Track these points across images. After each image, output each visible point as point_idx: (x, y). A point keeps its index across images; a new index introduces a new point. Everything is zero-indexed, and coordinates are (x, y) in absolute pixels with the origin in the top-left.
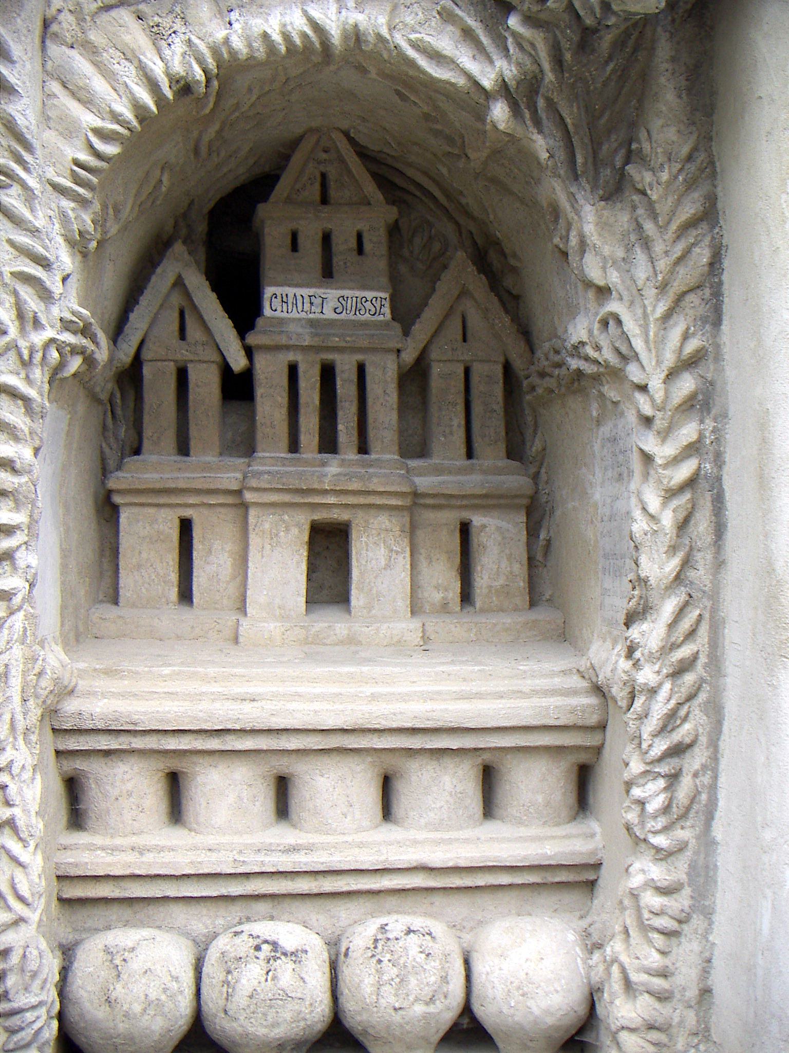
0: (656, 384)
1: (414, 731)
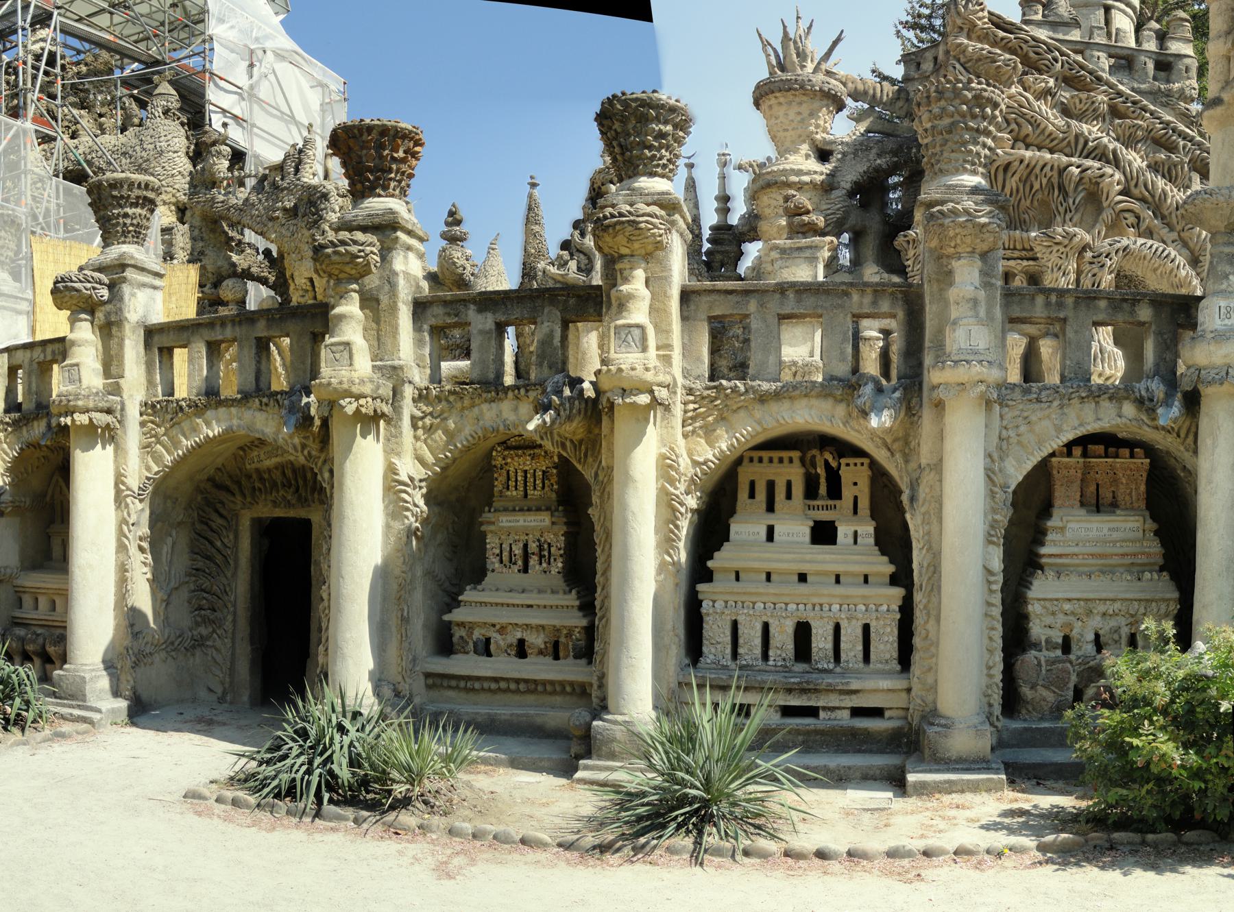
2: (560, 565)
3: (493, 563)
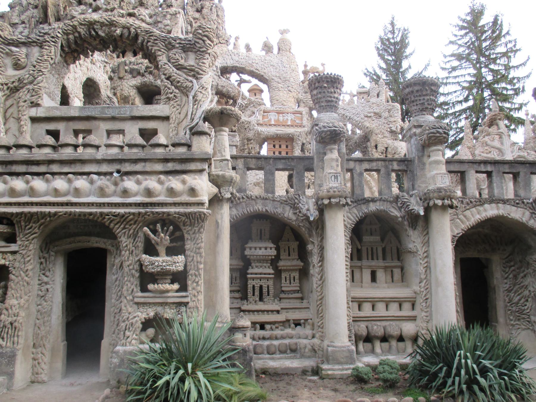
0: (422, 254)
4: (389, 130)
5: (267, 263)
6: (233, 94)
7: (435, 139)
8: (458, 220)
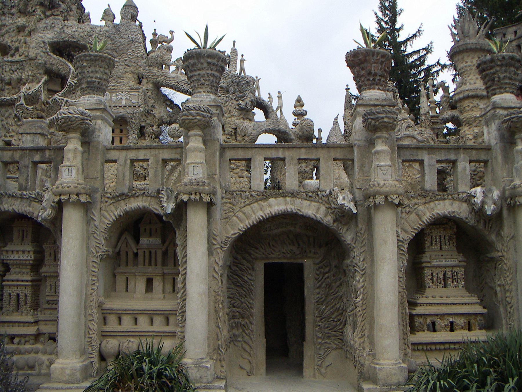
1: (154, 310)
2: (463, 283)
3: (429, 283)
4: (237, 107)
5: (26, 268)
6: (64, 72)
7: (190, 122)
8: (235, 218)
